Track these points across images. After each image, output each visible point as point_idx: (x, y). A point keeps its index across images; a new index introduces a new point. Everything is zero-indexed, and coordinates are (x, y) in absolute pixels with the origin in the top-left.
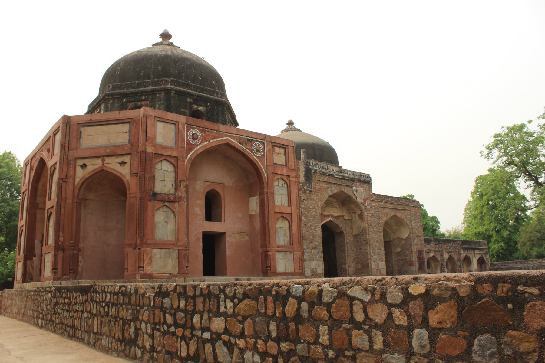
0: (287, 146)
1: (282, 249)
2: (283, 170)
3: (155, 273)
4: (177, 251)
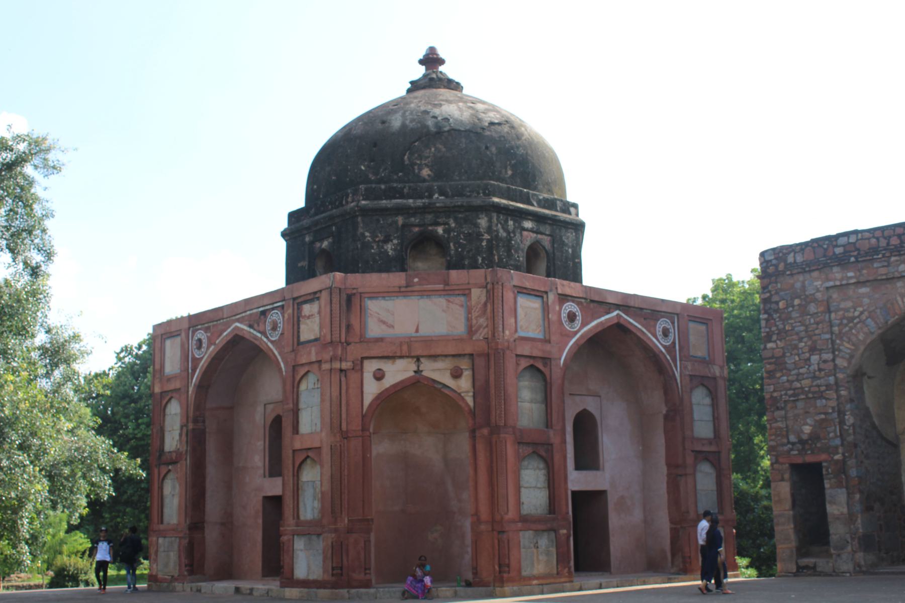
0: (321, 291)
1: (310, 530)
2: (309, 353)
3: (160, 576)
4: (178, 540)
